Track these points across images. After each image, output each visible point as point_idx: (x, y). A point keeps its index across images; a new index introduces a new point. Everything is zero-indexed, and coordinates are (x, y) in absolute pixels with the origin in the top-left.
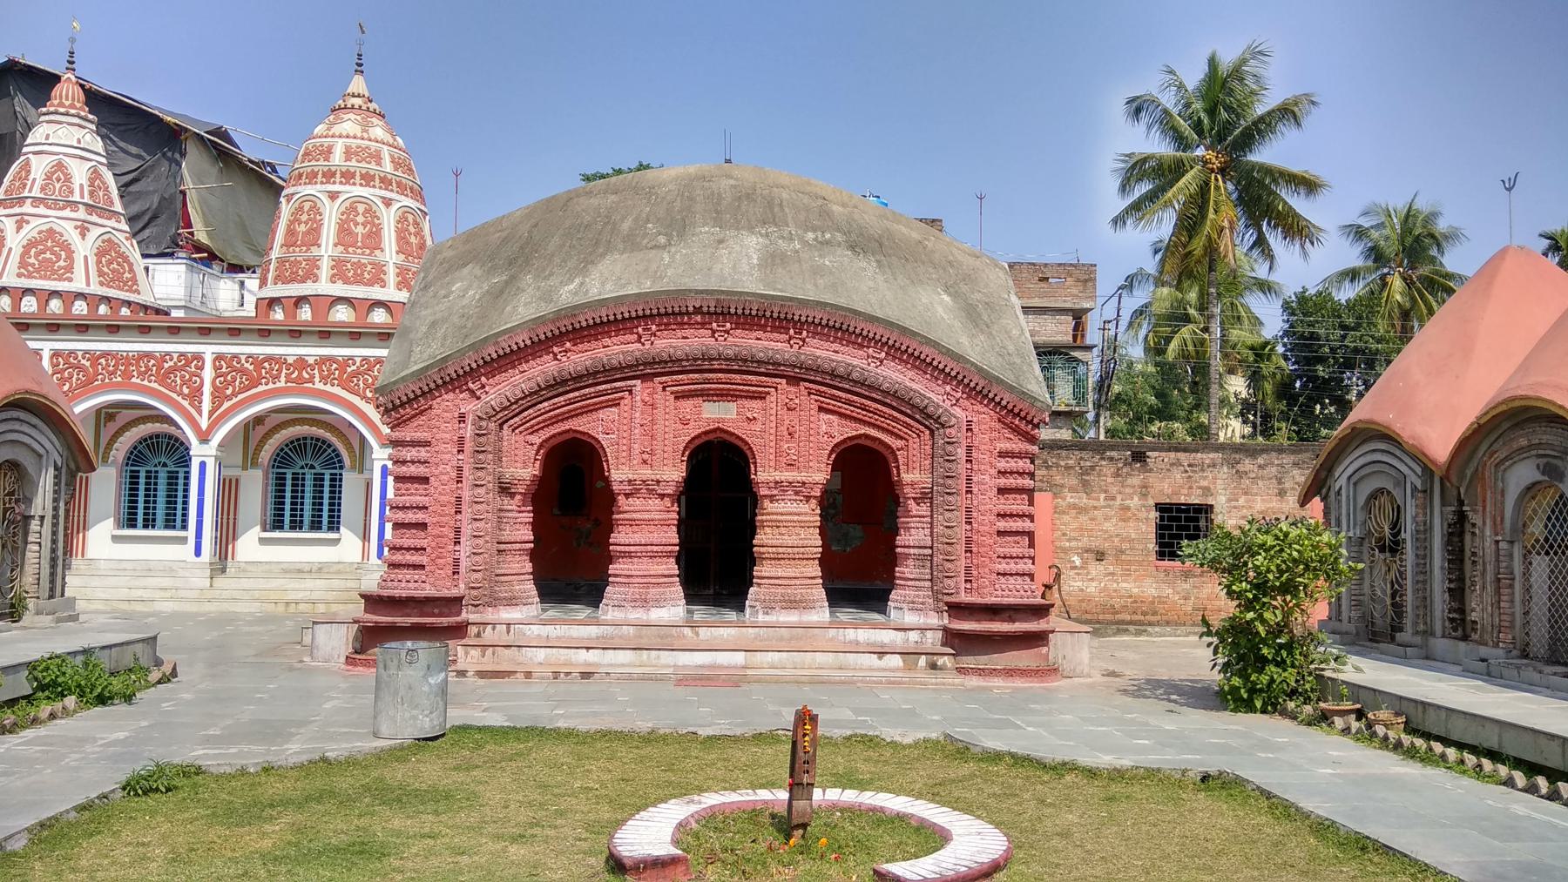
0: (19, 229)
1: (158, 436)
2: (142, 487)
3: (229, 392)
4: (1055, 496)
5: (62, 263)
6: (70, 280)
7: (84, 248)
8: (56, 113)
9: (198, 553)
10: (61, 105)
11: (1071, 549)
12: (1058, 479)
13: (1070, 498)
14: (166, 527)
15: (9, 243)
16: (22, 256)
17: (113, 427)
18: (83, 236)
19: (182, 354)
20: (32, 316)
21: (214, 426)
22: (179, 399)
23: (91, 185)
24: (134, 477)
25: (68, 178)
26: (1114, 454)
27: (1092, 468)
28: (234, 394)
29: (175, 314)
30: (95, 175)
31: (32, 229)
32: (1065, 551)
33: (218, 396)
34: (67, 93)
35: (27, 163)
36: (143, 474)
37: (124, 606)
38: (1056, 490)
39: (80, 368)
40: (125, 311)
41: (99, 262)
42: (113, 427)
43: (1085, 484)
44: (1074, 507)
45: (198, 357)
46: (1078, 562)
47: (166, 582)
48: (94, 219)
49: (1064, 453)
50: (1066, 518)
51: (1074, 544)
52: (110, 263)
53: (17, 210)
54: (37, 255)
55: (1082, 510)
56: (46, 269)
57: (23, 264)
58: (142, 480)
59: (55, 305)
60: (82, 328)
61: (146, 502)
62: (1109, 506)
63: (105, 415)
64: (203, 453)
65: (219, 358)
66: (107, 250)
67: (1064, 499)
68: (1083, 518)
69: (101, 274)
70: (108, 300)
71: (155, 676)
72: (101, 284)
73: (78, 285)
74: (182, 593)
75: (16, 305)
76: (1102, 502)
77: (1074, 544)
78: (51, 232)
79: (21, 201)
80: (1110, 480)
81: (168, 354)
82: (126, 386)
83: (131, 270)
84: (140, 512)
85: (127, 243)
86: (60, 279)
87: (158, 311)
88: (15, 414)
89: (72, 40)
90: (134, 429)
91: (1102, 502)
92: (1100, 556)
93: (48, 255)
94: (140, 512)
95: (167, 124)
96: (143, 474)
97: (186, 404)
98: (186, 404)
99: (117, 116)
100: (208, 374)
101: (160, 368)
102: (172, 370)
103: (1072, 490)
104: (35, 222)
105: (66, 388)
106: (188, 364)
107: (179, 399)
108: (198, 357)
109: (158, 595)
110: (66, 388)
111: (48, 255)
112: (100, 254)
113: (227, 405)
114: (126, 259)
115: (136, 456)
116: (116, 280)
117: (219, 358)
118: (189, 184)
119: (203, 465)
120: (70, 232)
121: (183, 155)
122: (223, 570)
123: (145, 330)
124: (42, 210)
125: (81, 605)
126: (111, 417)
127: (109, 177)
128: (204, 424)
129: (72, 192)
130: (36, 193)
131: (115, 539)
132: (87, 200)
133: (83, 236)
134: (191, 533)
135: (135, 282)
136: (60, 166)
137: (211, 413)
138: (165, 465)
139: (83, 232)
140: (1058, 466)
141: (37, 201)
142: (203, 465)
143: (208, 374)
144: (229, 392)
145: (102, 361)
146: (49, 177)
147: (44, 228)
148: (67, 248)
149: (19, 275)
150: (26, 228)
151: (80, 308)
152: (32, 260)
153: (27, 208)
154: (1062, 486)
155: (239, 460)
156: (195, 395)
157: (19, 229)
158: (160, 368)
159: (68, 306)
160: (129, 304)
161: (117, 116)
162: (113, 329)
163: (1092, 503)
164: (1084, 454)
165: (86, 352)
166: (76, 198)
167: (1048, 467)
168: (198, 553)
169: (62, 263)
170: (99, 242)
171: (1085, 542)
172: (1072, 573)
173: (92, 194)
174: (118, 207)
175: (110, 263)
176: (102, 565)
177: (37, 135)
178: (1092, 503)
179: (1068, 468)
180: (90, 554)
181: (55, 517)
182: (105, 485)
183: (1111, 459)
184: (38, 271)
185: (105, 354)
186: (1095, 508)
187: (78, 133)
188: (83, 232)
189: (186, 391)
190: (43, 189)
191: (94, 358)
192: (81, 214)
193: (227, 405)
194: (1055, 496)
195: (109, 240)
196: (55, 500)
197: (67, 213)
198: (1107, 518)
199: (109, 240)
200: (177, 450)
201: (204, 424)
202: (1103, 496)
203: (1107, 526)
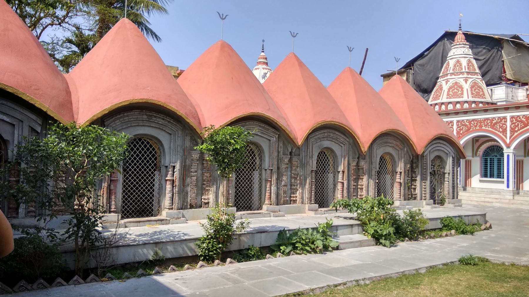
0: (447, 83)
1: (493, 146)
2: (489, 164)
3: (516, 129)
5: (460, 92)
6: (462, 97)
7: (466, 86)
8: (456, 45)
9: (508, 187)
10: (458, 42)
14: (498, 177)
15: (444, 89)
16: (448, 92)
17: (478, 144)
18: (466, 82)
19: (499, 118)
20: (451, 110)
21: (512, 142)
22: (499, 133)
23: (468, 65)
24: (486, 160)
25: (461, 65)
28: (519, 130)
29: (498, 104)
30: (469, 62)
31: (450, 84)
33: (513, 131)
34: (460, 37)
35: (448, 63)
36: (489, 159)
37: (483, 204)
39: (465, 125)
40: (481, 105)
41: (471, 90)
42: (478, 144)
45: (505, 118)
47: (497, 196)
48: (470, 76)
52: (475, 90)
53: (446, 78)
54: (452, 91)
56: (455, 95)
57: (448, 94)
58: (489, 162)
59: (458, 106)
60: (466, 112)
61: (490, 169)
63: (475, 140)
64: (508, 152)
65: (512, 117)
66: (474, 86)
69: (472, 94)
70: (474, 102)
71: (483, 227)
72: (473, 97)
73: (465, 98)
74: (503, 201)
75: (446, 108)
78: (456, 83)
79: (447, 75)
81: (494, 118)
82: (480, 130)
83: (483, 91)
84: (489, 172)
85: (481, 82)
86: (460, 97)
87: (492, 104)
88: (441, 142)
89: (460, 20)
90: (490, 143)
93: (455, 90)
94: (489, 172)
95: (496, 39)
96: (489, 159)
97: (501, 135)
98: (501, 135)
99: (474, 40)
100: (508, 123)
101: (491, 123)
102: (496, 123)
104: (451, 81)
105: (461, 132)
106: (501, 121)
107: (499, 133)
108: (505, 118)
109: (495, 200)
110: (461, 132)
111: (455, 90)
112: (472, 87)
113: (516, 134)
114: (480, 88)
115: (486, 153)
116: (478, 95)
117: (512, 117)
118: (505, 58)
119: (508, 156)
120: (462, 82)
121: (502, 48)
122: (518, 193)
123: (486, 111)
124: (453, 77)
125: (463, 202)
126: (477, 141)
127: (474, 61)
128: (508, 141)
129: (462, 69)
130: (451, 71)
131: (481, 181)
132: (467, 70)
133: (466, 82)
134: (505, 179)
135: (484, 94)
136: (458, 61)
137: (510, 138)
138: (496, 156)
139: (466, 81)
141: (452, 74)
142: (508, 156)
143: (508, 123)
144: (516, 129)
145: (472, 122)
146: (455, 66)
147: (454, 82)
148: (461, 88)
149: (447, 98)
150: (449, 83)
151: (466, 106)
152: (451, 93)
153: (449, 77)
155: (523, 154)
156: (504, 131)
157: (447, 83)
158: (491, 123)
159: (462, 106)
160: (482, 102)
161: (474, 40)
162: (475, 112)
165: (467, 120)
166: (464, 70)
168: (508, 187)
169: (460, 92)
170: (471, 84)
173: (468, 68)
174: (477, 71)
175: (475, 90)
176: (477, 190)
177: (451, 53)
180: (473, 186)
181: (453, 173)
182: (477, 164)
184: (452, 96)
185: (473, 120)
187: (463, 49)
188: (466, 81)
189: (501, 130)
190: (453, 70)
191: (470, 122)
192: (465, 75)
193: (516, 134)
195: (475, 82)
196: (453, 168)
197: (461, 76)
199: (475, 82)
200: (499, 150)
201: (508, 141)
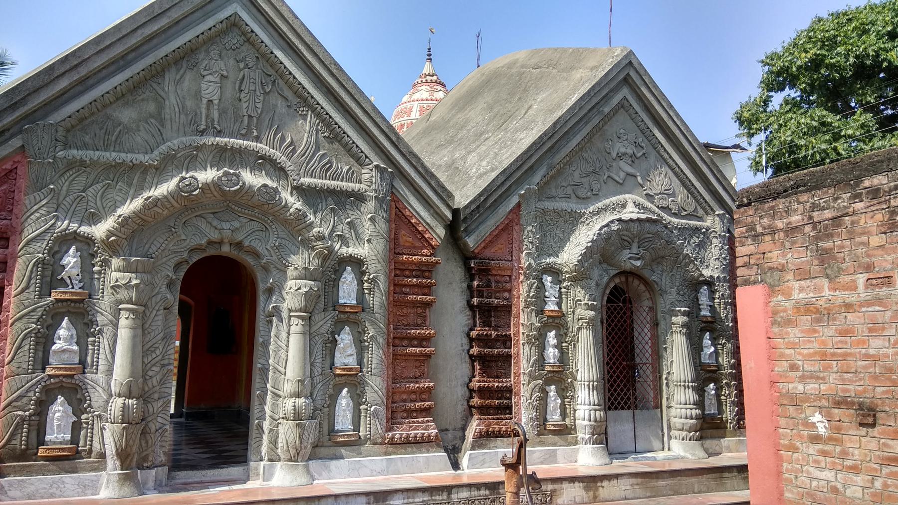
4: (772, 290)
11: (806, 397)
12: (776, 257)
13: (799, 292)
26: (879, 180)
27: (836, 220)
32: (797, 401)
38: (771, 277)
43: (825, 258)
44: (807, 308)
46: (822, 429)
49: (781, 204)
50: (794, 333)
51: (812, 387)
55: (821, 314)
62: (878, 301)
67: (788, 295)
68: (827, 332)
76: (862, 293)
77: (812, 387)
80: (875, 241)
91: (862, 293)
92: (868, 416)
103: (803, 274)
140: (772, 231)
154: (782, 269)
163: (842, 296)
164: (820, 197)
167: (756, 238)
171: (832, 384)
172: (813, 449)
178: (842, 296)
179: (791, 231)
183: (875, 193)
186: (848, 307)
194: (772, 290)
198: (875, 329)
202: (861, 279)
203: (876, 345)
